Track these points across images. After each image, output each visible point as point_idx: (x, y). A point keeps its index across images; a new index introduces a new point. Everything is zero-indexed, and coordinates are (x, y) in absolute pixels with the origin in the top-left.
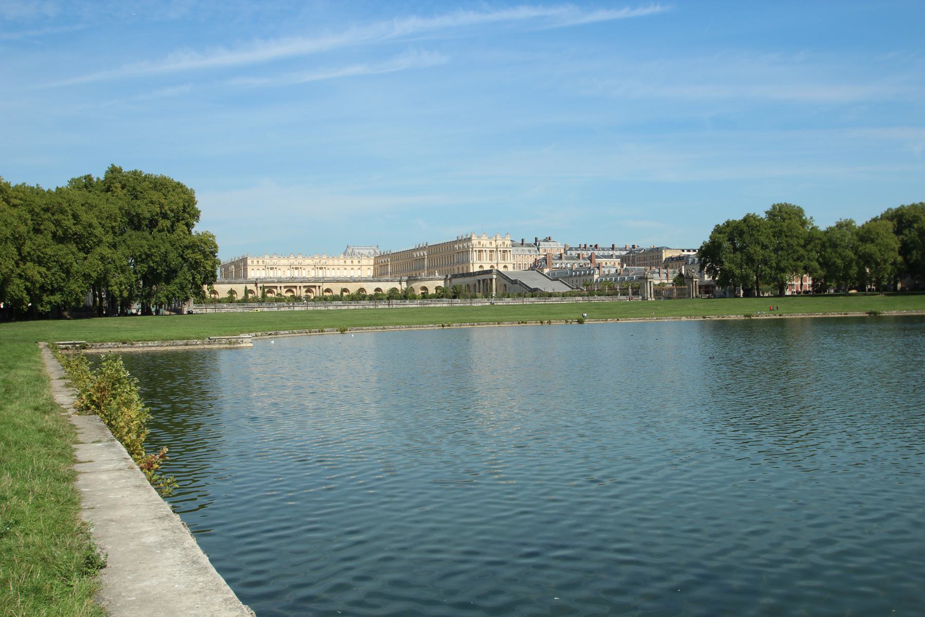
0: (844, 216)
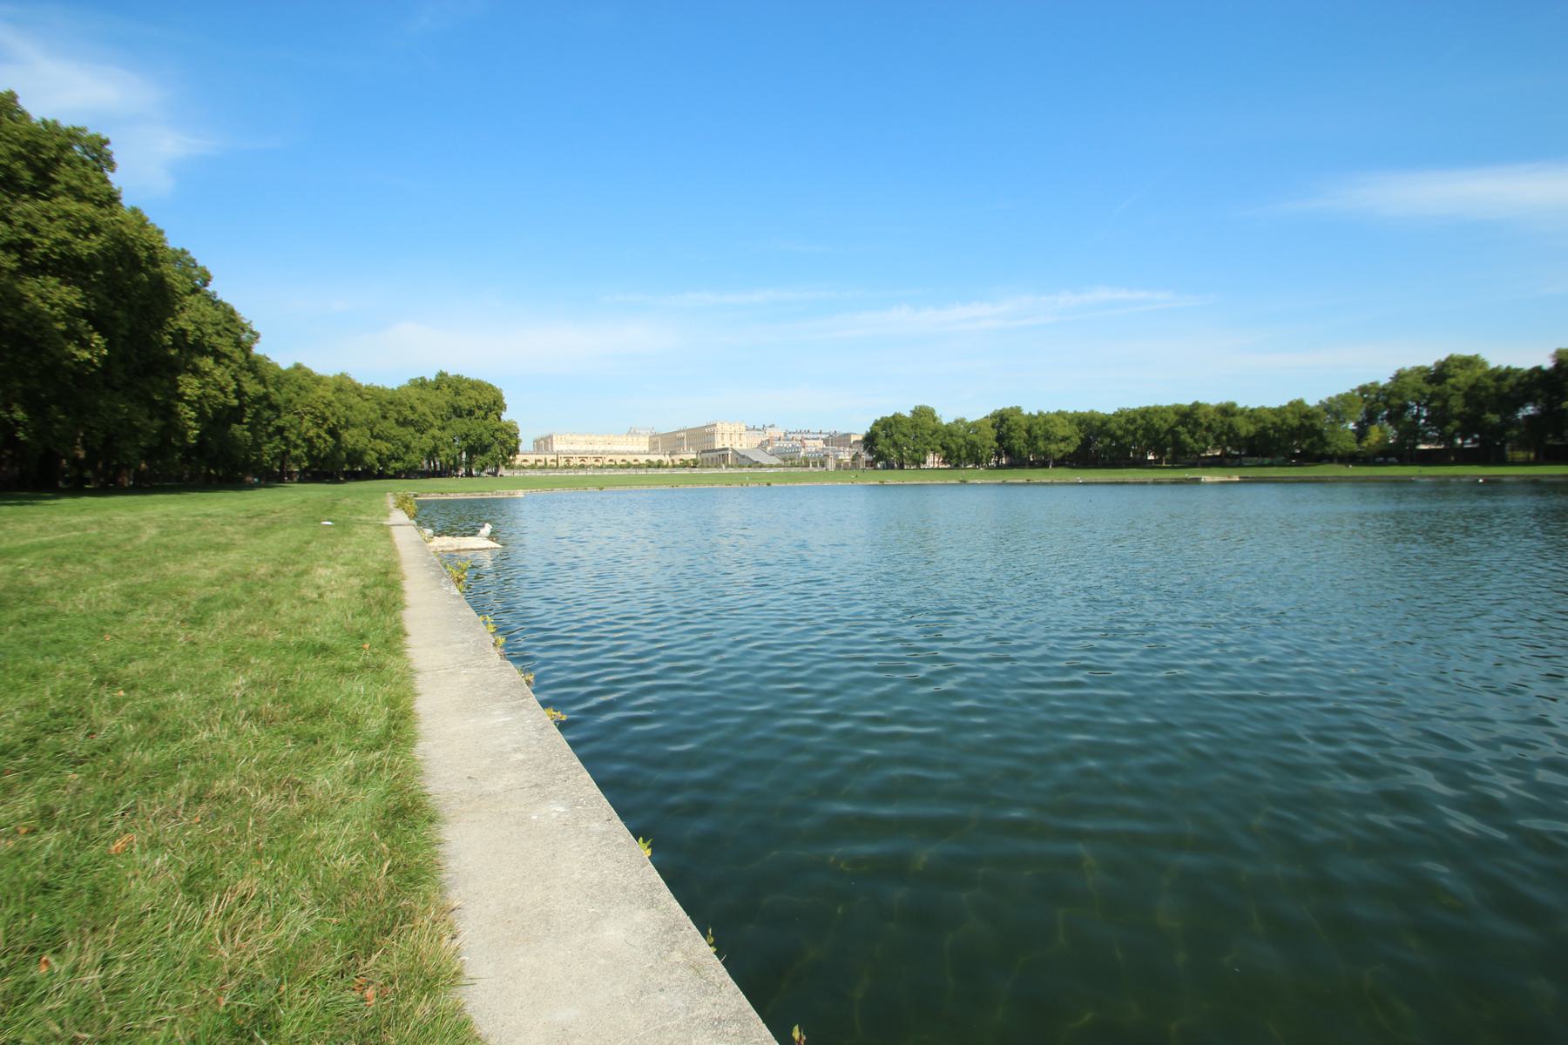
0: (959, 416)
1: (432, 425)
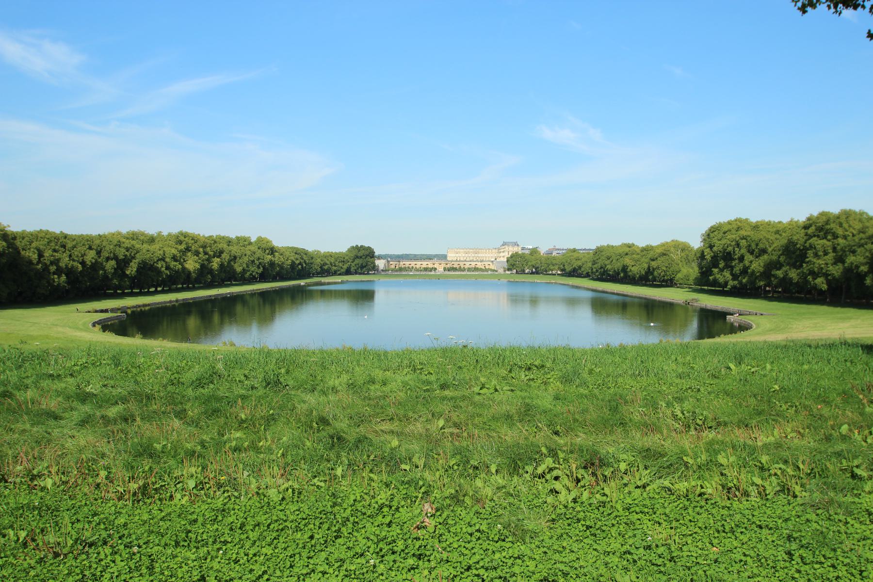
1: (349, 262)
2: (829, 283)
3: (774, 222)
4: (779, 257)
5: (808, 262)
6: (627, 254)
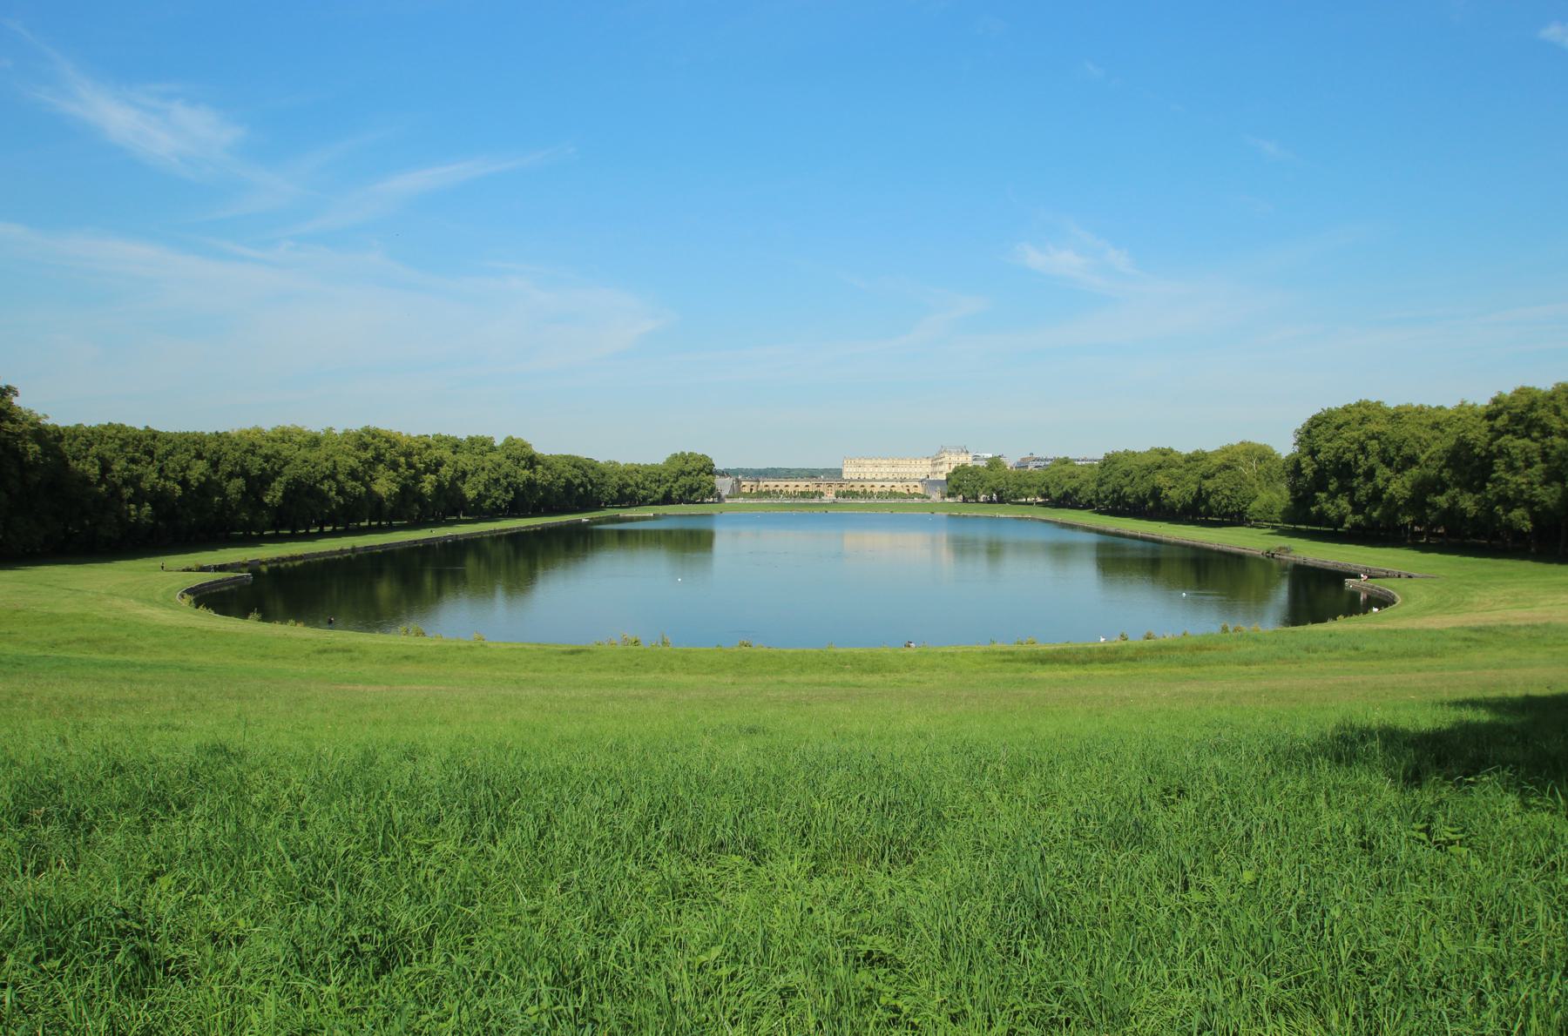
2: (1535, 518)
3: (1430, 407)
4: (1441, 471)
5: (1494, 481)
6: (1159, 467)
